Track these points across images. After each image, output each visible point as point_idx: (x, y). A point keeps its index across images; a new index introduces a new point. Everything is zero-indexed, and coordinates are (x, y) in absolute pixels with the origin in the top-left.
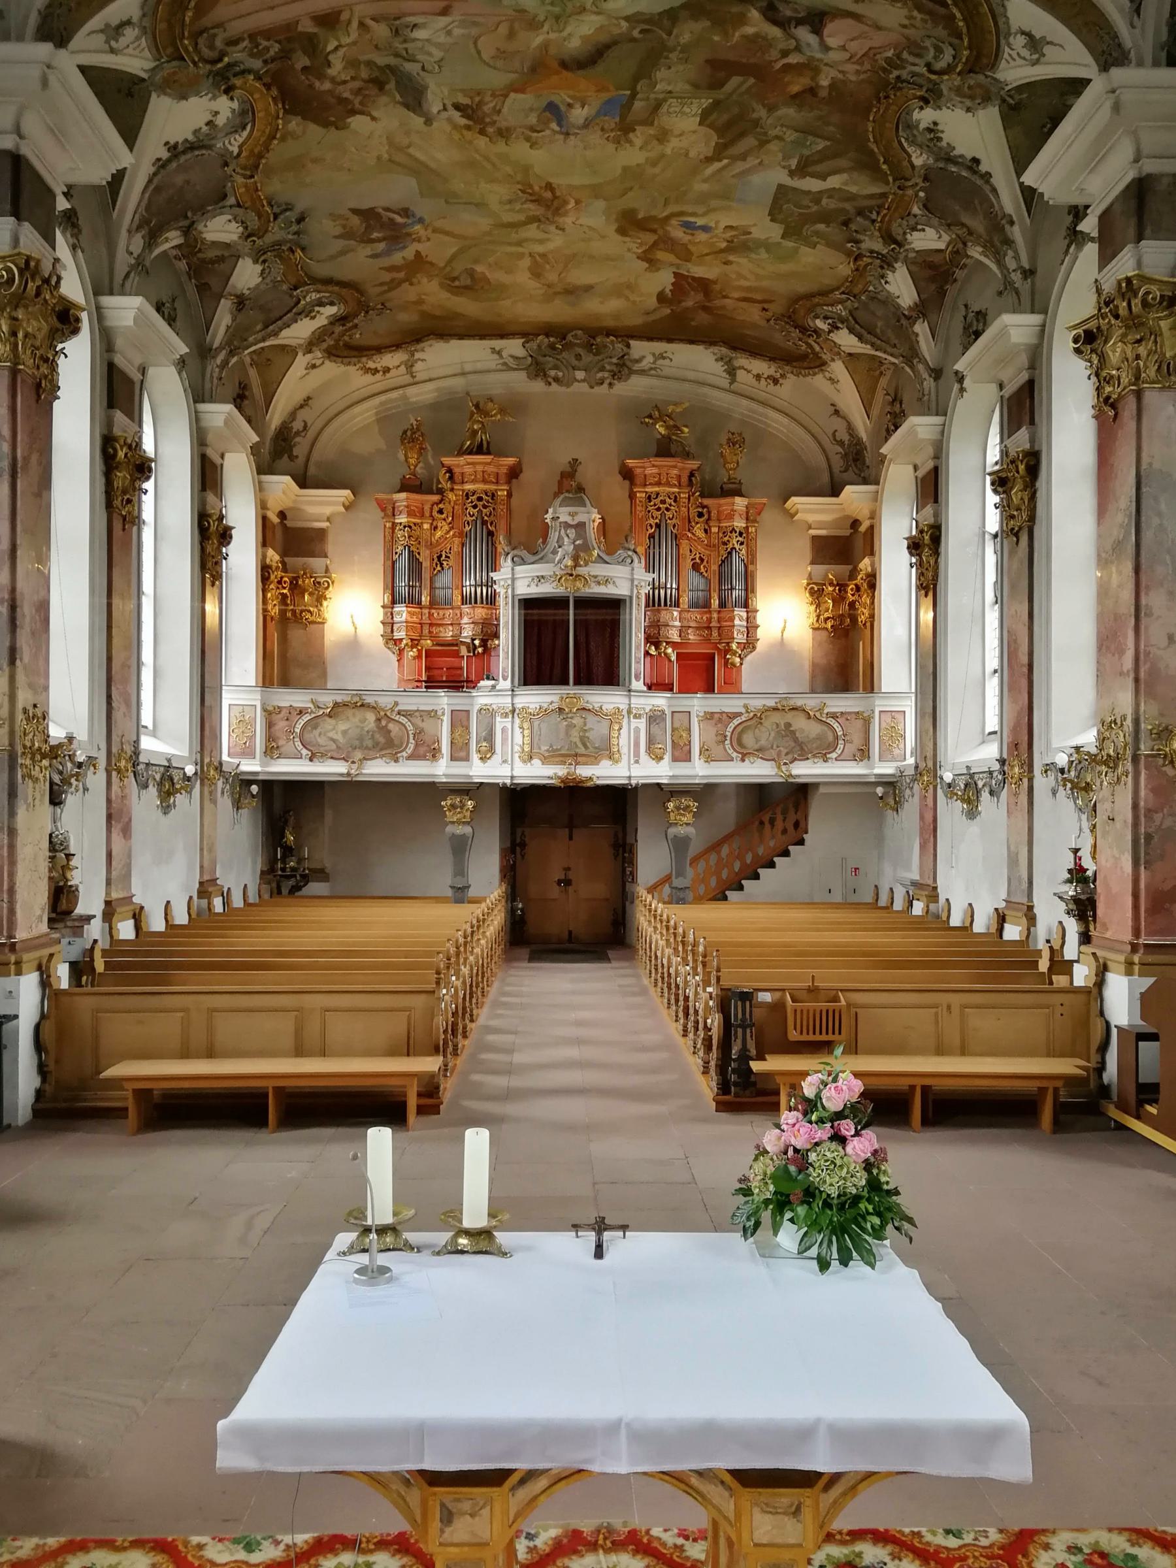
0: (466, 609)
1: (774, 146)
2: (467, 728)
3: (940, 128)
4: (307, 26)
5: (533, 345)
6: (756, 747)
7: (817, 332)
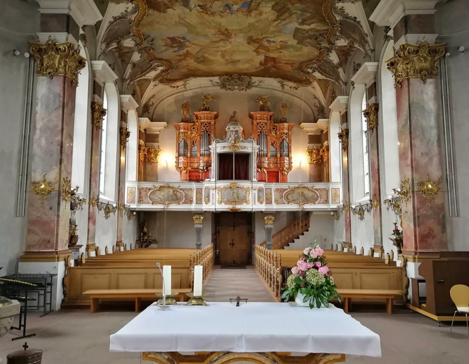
0: (201, 158)
1: (294, 16)
2: (201, 194)
3: (344, 8)
5: (222, 78)
6: (293, 199)
7: (308, 73)
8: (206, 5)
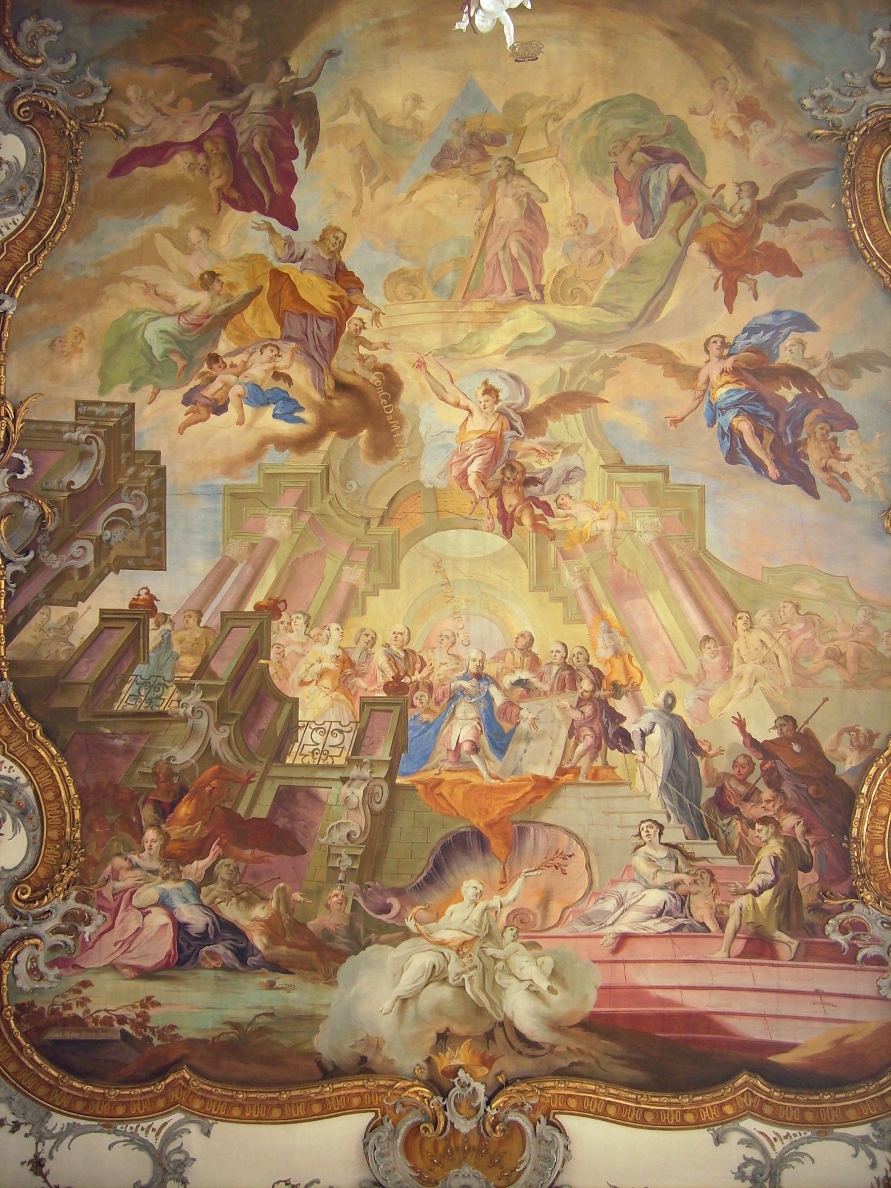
1: (189, 662)
8: (595, 749)
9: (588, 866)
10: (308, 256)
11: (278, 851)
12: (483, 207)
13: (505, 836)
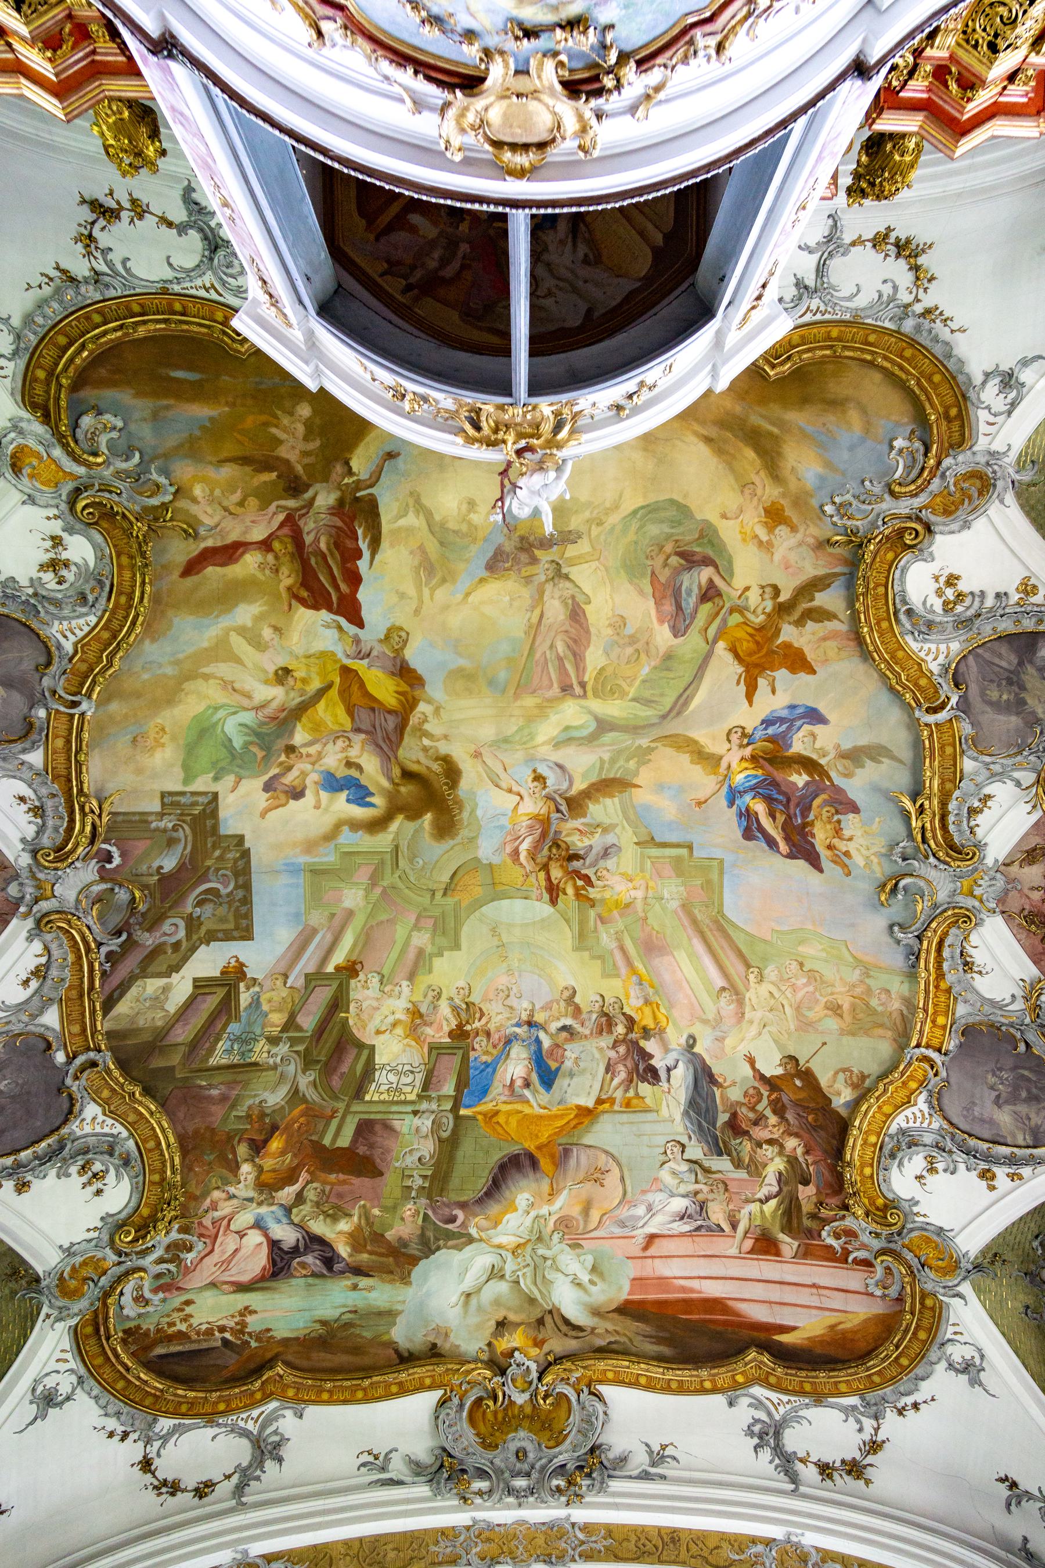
1: (278, 1019)
4: (788, 1244)
9: (622, 1179)
10: (374, 653)
11: (359, 1174)
12: (533, 608)
13: (552, 1156)
